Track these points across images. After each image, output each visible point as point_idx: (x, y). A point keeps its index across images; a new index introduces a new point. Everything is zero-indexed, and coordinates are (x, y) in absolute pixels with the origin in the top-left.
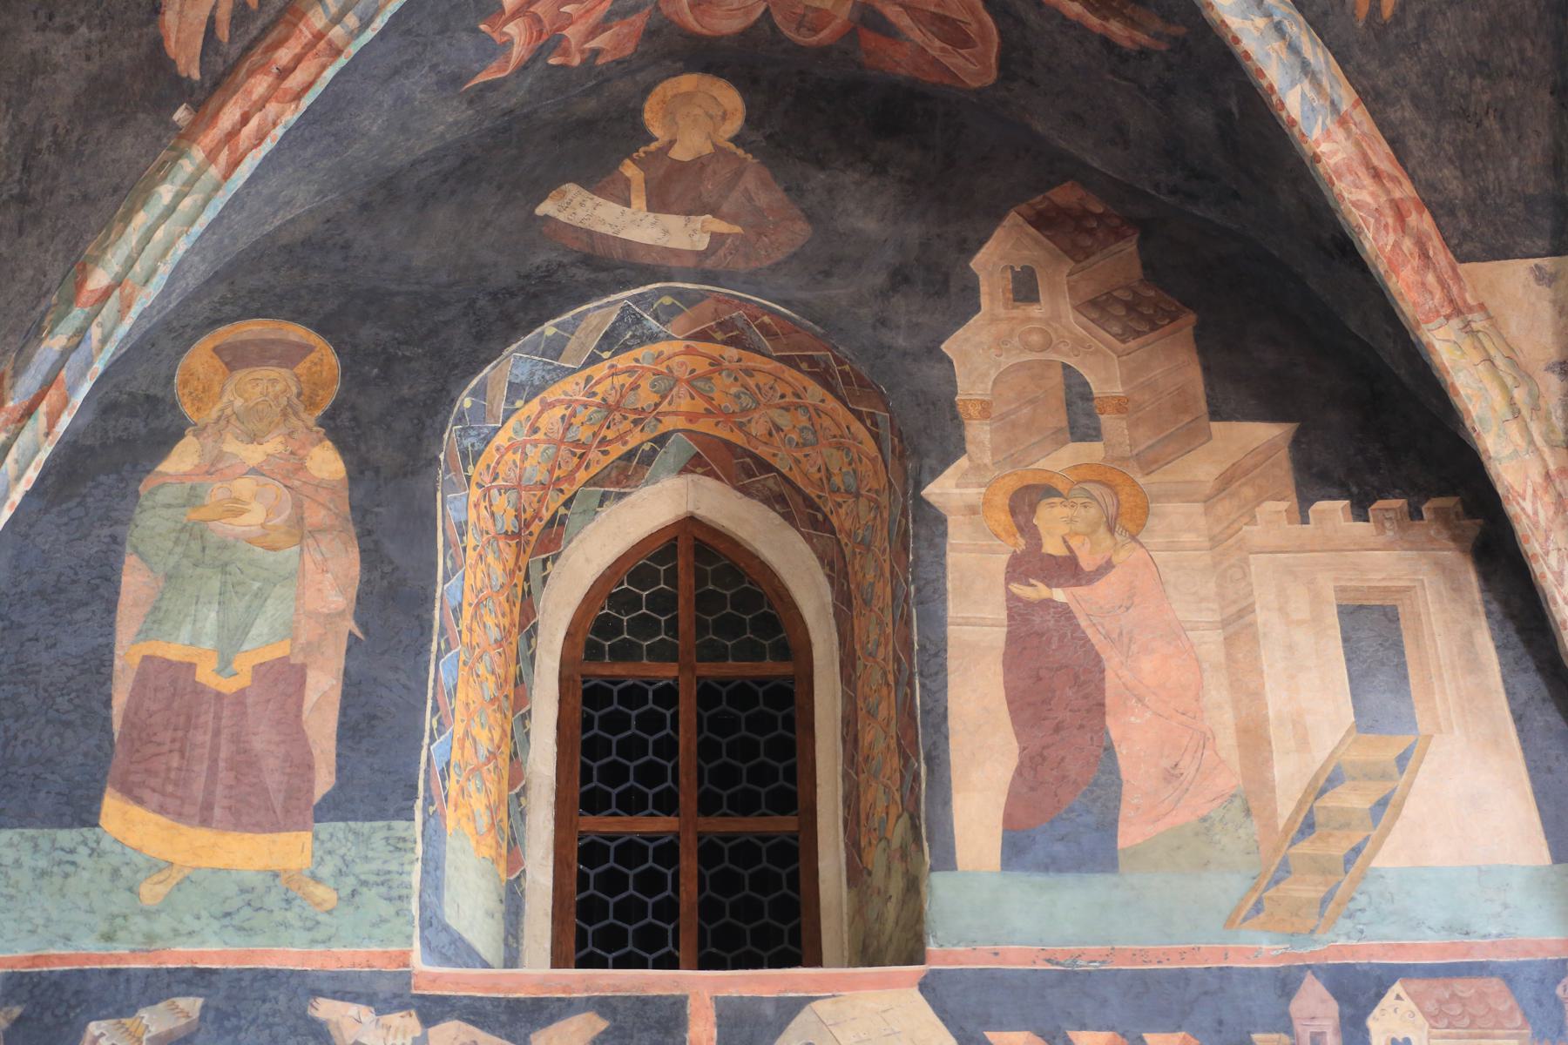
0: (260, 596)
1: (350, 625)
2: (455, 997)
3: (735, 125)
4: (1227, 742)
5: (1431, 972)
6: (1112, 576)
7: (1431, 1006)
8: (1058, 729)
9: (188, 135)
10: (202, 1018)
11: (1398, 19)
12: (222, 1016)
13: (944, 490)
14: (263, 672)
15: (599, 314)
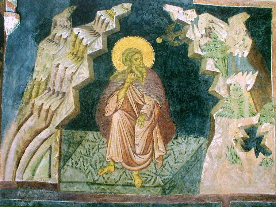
2: (206, 5)
10: (132, 10)
12: (137, 10)
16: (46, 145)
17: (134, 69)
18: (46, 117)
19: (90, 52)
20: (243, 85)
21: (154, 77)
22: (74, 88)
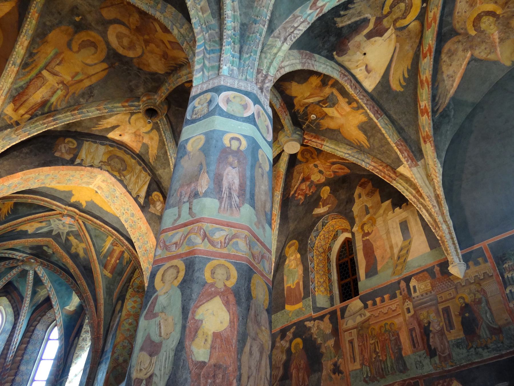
0: (295, 275)
1: (303, 275)
5: (417, 274)
6: (373, 232)
7: (417, 279)
8: (369, 256)
11: (371, 146)
14: (296, 284)
15: (320, 224)
19: (285, 349)
20: (330, 345)
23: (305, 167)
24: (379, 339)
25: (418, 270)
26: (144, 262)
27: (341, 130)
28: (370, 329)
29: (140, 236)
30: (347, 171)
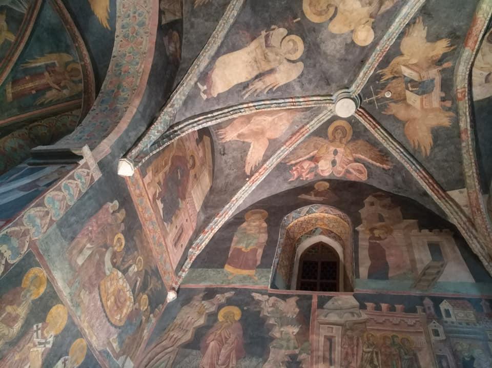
1: (265, 244)
3: (328, 187)
4: (408, 262)
7: (453, 304)
9: (247, 181)
11: (430, 155)
13: (358, 228)
14: (251, 250)
15: (306, 209)
16: (167, 356)
17: (228, 320)
18: (173, 342)
19: (207, 312)
21: (239, 325)
22: (194, 328)
23: (325, 146)
24: (380, 351)
25: (453, 295)
26: (111, 83)
27: (407, 125)
28: (365, 335)
29: (130, 53)
30: (363, 178)
